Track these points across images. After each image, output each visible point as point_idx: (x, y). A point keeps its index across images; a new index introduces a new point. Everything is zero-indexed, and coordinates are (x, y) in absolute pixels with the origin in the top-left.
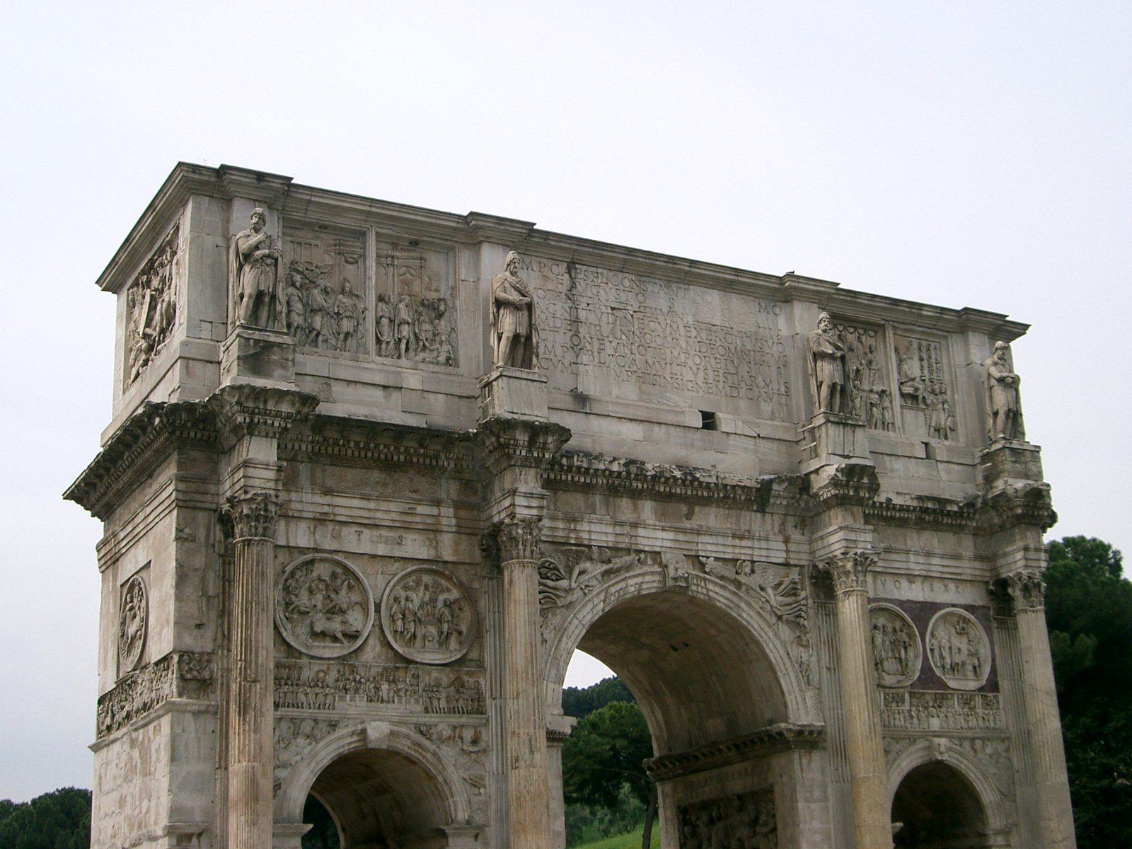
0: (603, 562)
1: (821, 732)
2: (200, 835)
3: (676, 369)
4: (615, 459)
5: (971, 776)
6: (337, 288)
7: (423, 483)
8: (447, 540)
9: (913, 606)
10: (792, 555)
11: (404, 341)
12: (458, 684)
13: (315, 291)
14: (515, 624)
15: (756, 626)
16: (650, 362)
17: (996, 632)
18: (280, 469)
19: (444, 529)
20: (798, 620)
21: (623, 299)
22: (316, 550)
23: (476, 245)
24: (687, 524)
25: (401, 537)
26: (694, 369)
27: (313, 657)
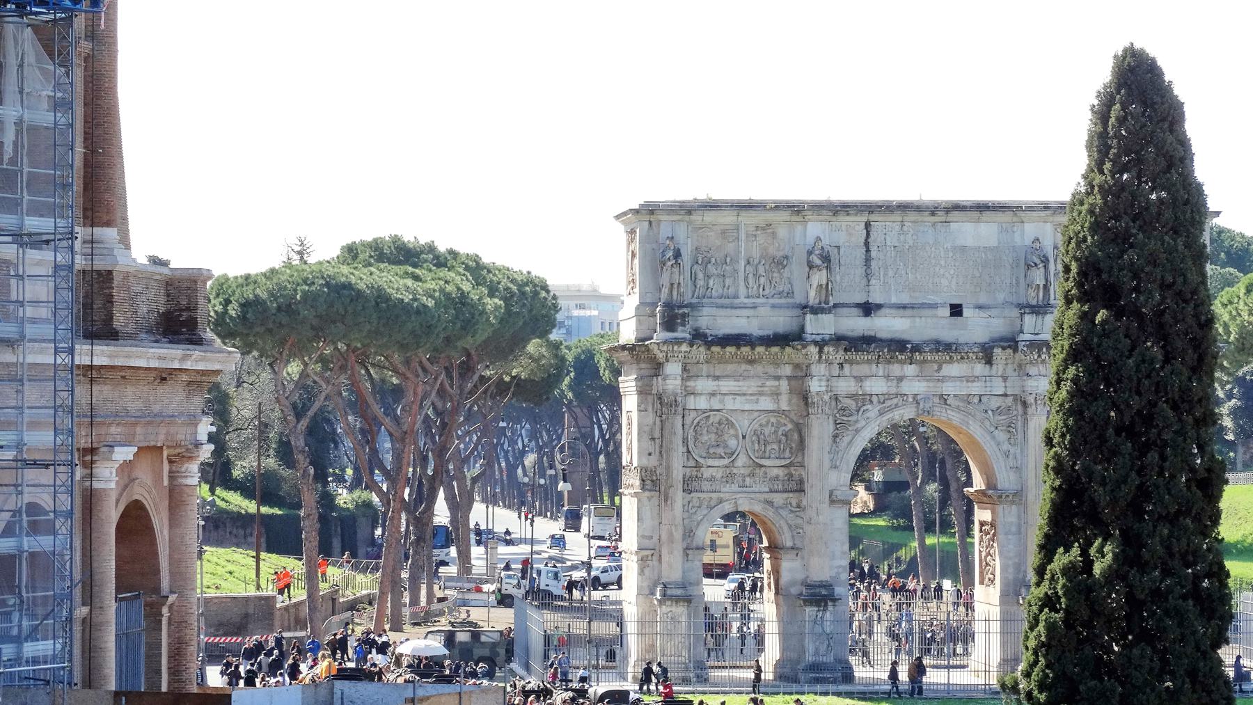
0: (879, 402)
1: (1015, 495)
2: (652, 555)
7: (771, 370)
13: (709, 266)
15: (979, 434)
16: (919, 277)
18: (682, 379)
22: (711, 411)
25: (757, 399)
26: (950, 277)
27: (710, 466)
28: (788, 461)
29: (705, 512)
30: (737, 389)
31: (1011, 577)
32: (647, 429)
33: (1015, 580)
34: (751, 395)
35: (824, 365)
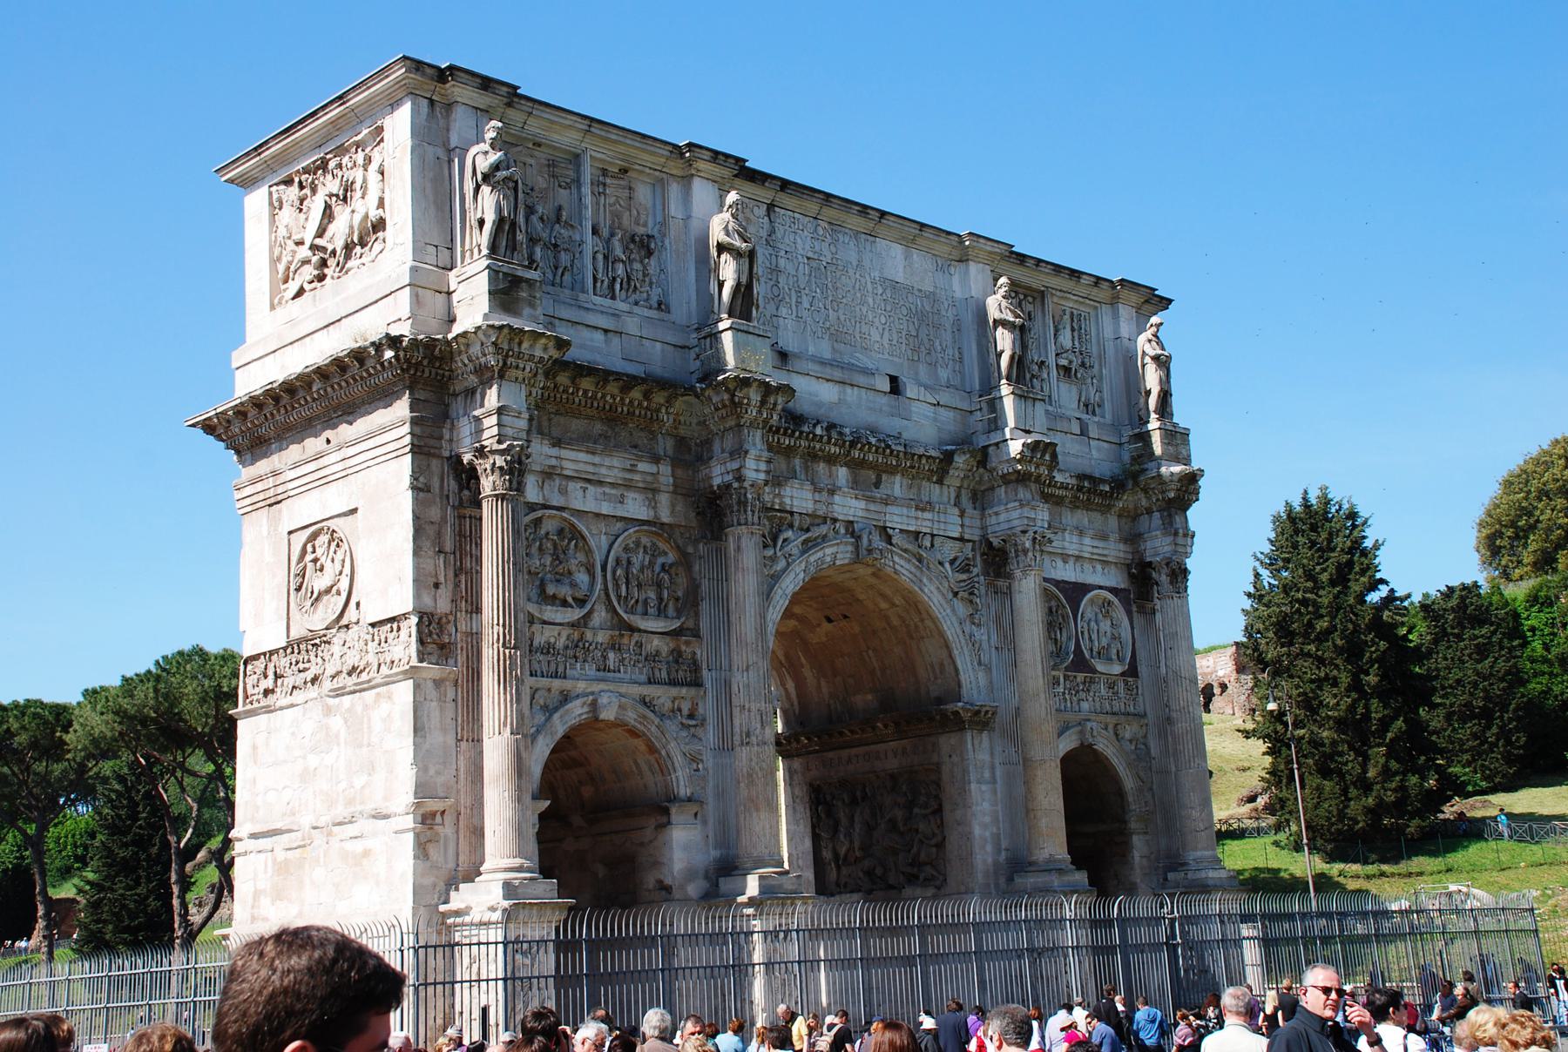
0: (802, 529)
2: (443, 812)
3: (865, 329)
4: (818, 422)
5: (1115, 761)
6: (553, 217)
7: (641, 438)
8: (664, 499)
9: (1067, 586)
10: (967, 530)
11: (619, 280)
12: (677, 654)
14: (744, 593)
15: (936, 602)
16: (842, 318)
17: (1135, 615)
19: (663, 488)
20: (971, 597)
21: (817, 249)
22: (545, 507)
23: (686, 180)
24: (877, 494)
27: (545, 622)
28: (676, 624)
29: (540, 718)
30: (591, 469)
31: (990, 860)
32: (431, 530)
33: (996, 864)
34: (613, 485)
35: (759, 433)
